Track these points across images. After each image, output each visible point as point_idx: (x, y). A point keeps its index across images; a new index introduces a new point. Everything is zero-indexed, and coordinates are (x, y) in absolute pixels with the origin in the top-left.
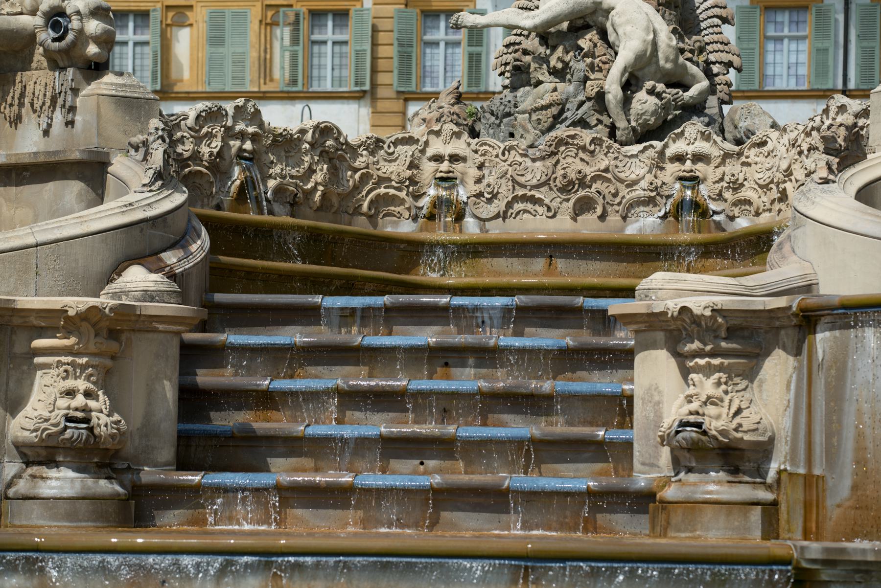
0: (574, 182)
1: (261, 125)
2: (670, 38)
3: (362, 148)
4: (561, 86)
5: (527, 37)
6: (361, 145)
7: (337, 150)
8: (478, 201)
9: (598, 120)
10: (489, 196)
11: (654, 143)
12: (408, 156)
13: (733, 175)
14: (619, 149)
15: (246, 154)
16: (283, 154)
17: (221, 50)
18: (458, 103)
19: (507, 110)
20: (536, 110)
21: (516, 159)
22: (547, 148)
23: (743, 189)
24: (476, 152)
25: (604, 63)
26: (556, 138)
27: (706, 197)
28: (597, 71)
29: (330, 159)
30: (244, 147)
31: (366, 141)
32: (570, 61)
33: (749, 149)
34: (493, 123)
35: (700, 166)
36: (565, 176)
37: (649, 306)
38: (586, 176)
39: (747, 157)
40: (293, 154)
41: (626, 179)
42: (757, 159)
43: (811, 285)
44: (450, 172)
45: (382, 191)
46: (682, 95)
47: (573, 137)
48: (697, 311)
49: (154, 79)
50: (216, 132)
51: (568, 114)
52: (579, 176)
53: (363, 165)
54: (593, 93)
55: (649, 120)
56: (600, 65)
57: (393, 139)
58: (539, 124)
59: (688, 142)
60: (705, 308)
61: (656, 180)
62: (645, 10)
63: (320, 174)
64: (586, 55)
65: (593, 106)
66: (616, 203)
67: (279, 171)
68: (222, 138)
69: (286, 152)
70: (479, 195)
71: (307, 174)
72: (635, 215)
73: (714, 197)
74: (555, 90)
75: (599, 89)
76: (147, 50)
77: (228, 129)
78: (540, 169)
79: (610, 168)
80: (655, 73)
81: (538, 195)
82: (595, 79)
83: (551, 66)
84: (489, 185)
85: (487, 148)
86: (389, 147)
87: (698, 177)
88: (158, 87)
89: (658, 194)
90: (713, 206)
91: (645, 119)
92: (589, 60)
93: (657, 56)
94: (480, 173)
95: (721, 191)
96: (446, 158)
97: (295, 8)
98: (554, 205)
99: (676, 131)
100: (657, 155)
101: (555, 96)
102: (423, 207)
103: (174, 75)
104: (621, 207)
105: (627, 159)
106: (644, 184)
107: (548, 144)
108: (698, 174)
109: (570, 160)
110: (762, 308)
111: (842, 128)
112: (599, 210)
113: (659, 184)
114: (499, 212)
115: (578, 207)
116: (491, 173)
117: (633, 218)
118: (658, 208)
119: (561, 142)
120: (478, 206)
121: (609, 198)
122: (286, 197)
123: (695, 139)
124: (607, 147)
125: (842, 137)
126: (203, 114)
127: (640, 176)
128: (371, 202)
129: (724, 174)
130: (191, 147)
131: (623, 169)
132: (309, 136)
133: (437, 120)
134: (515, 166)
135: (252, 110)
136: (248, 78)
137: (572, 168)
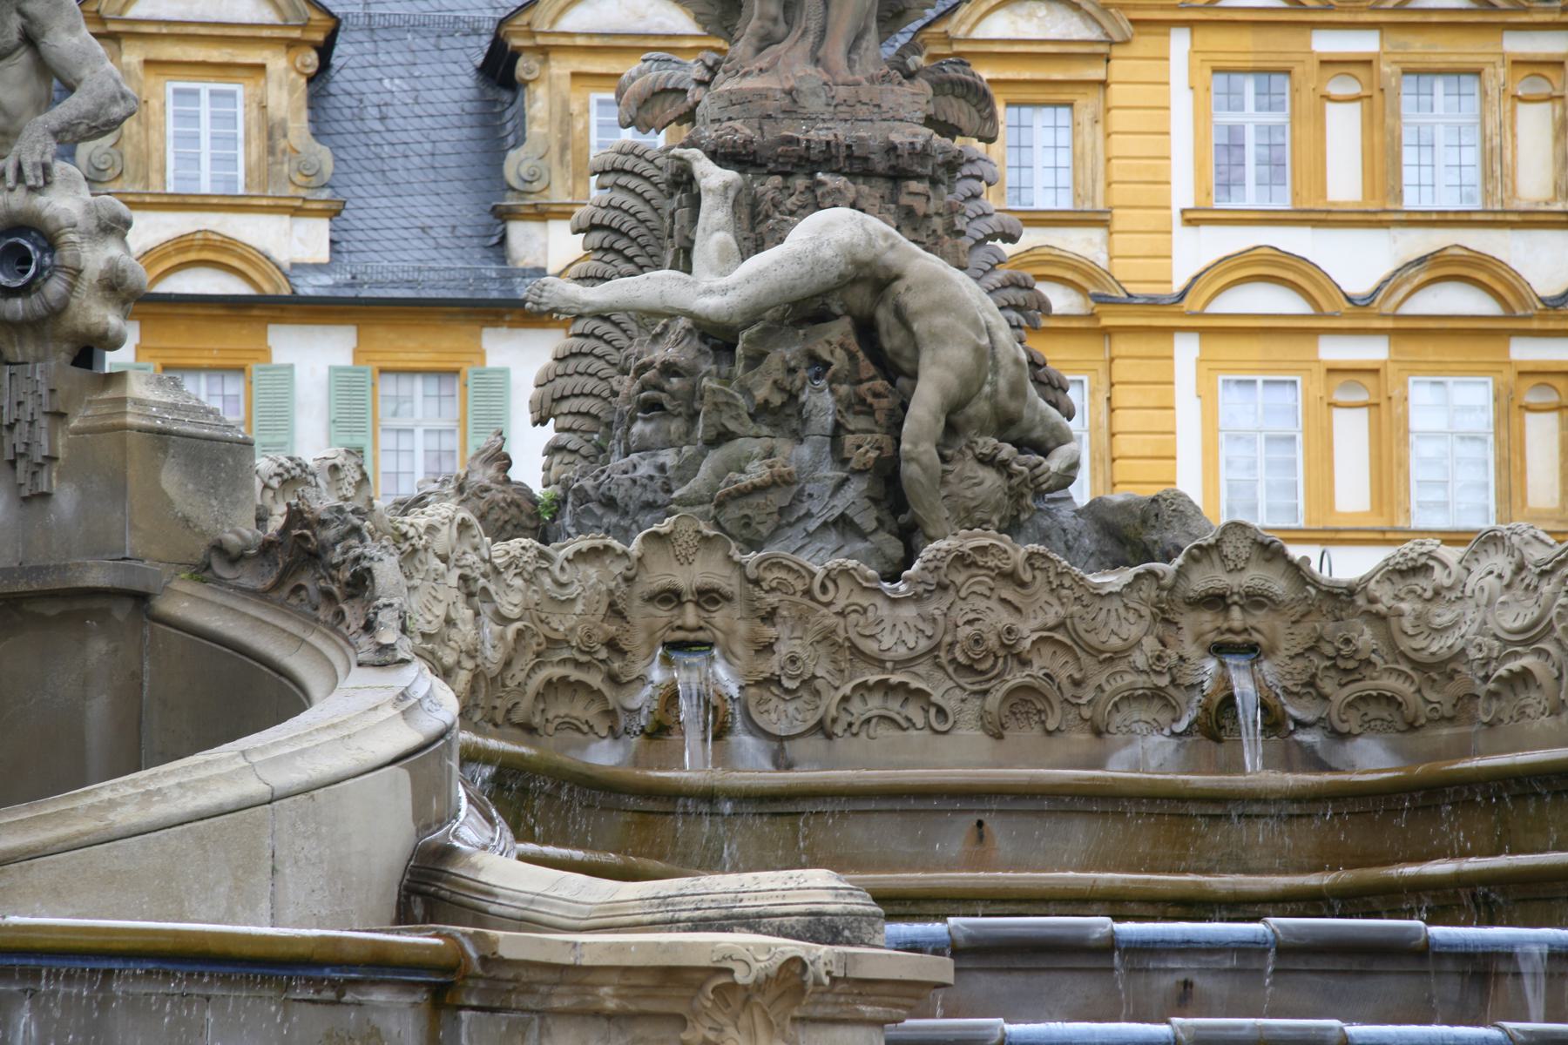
3: (512, 571)
4: (784, 446)
5: (656, 338)
6: (510, 564)
8: (767, 695)
9: (878, 519)
11: (1158, 566)
19: (649, 497)
27: (1278, 691)
29: (470, 595)
32: (802, 388)
35: (1260, 619)
36: (978, 641)
41: (1101, 647)
44: (701, 628)
45: (556, 672)
47: (982, 550)
56: (870, 399)
57: (569, 551)
61: (1168, 651)
65: (869, 488)
70: (773, 681)
73: (1295, 689)
74: (770, 454)
81: (915, 684)
84: (793, 660)
85: (783, 574)
87: (1257, 644)
89: (1173, 682)
92: (844, 389)
95: (1314, 676)
98: (950, 705)
105: (1098, 604)
106: (1140, 660)
107: (931, 565)
108: (1257, 637)
109: (982, 604)
113: (1174, 660)
117: (1119, 736)
119: (962, 560)
120: (766, 708)
129: (1320, 638)
134: (854, 616)
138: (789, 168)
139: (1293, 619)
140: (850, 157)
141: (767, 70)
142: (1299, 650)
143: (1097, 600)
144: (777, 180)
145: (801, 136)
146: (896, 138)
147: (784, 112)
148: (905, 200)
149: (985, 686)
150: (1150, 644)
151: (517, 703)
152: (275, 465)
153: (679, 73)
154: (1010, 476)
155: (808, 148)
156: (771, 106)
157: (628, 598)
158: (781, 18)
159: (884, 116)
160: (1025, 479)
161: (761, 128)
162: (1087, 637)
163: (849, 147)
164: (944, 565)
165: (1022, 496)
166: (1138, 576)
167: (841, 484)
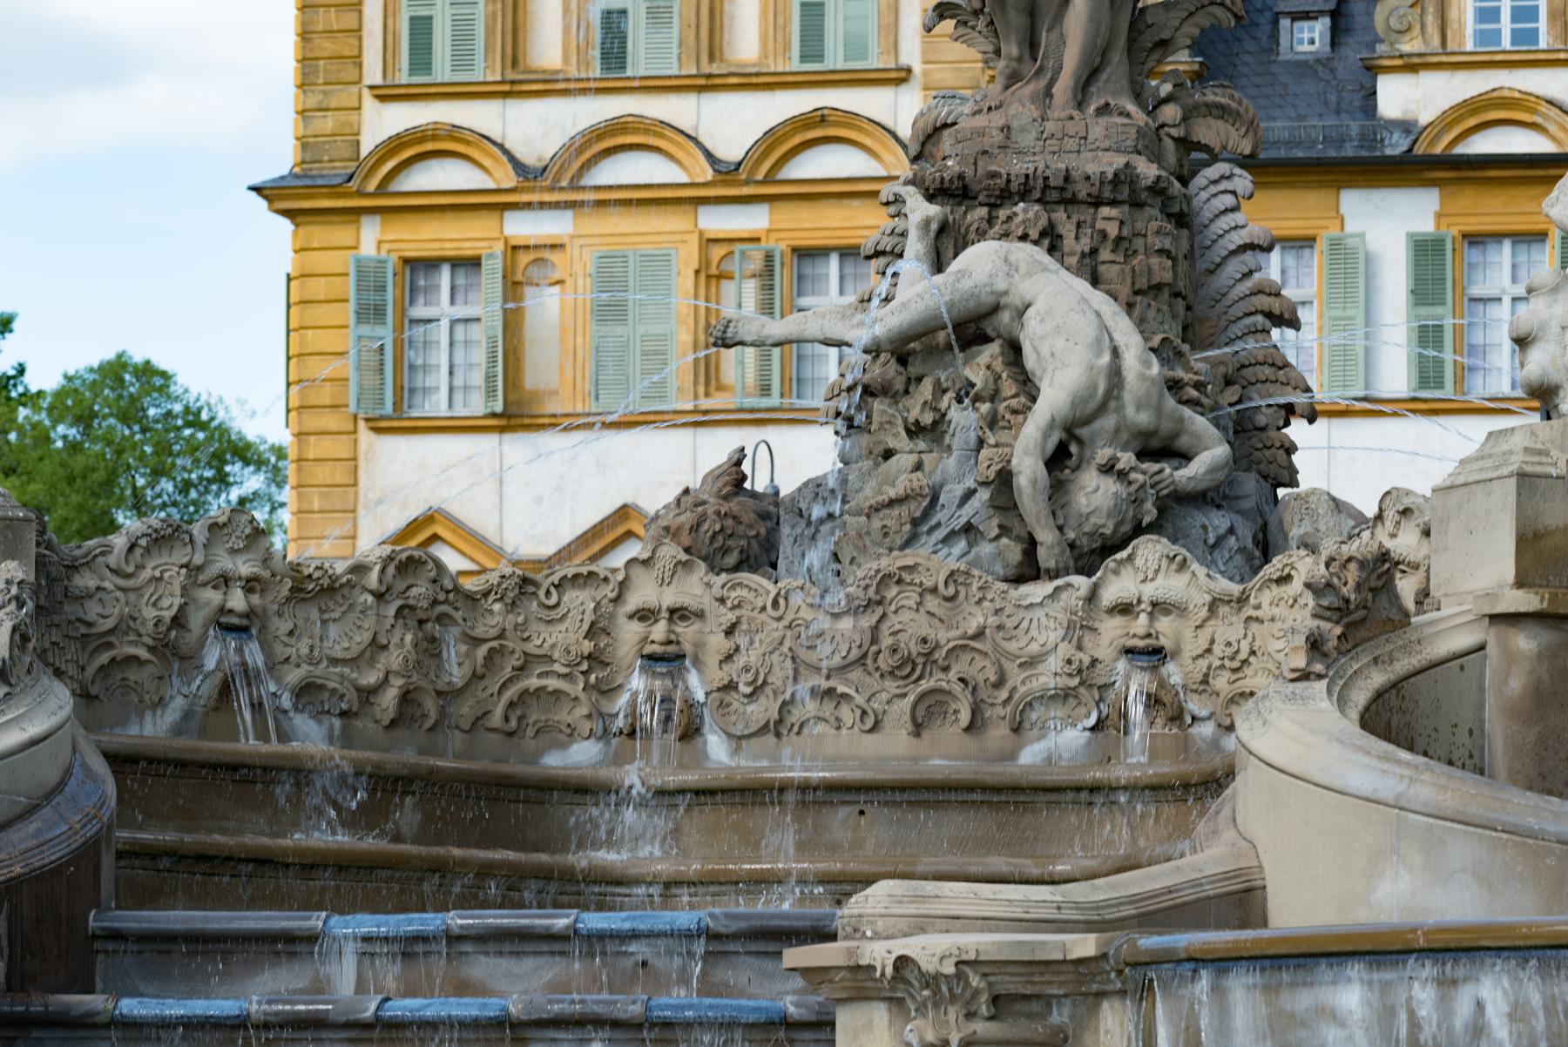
0: (913, 662)
1: (267, 560)
2: (1147, 364)
3: (492, 597)
6: (489, 592)
7: (435, 602)
9: (1000, 526)
10: (748, 690)
12: (588, 613)
13: (1229, 644)
14: (1003, 592)
15: (235, 621)
16: (314, 614)
17: (620, 330)
18: (737, 494)
20: (877, 509)
21: (801, 614)
22: (861, 593)
23: (1248, 671)
24: (722, 601)
25: (1015, 412)
26: (878, 571)
28: (1004, 428)
29: (421, 622)
30: (231, 604)
31: (499, 584)
33: (1260, 590)
34: (802, 534)
35: (1165, 624)
37: (851, 953)
38: (937, 646)
39: (1258, 607)
40: (333, 615)
41: (1018, 653)
42: (1276, 611)
43: (1248, 890)
44: (670, 642)
45: (533, 682)
46: (1172, 475)
48: (929, 965)
49: (490, 392)
50: (170, 577)
51: (940, 516)
52: (926, 649)
53: (493, 632)
54: (991, 474)
55: (1103, 526)
56: (1008, 416)
57: (556, 578)
58: (886, 535)
59: (1142, 577)
60: (942, 959)
61: (1081, 655)
62: (1096, 306)
63: (395, 654)
64: (977, 399)
66: (999, 700)
67: (305, 651)
68: (184, 588)
69: (322, 611)
70: (730, 687)
71: (368, 654)
72: (1039, 724)
73: (1195, 687)
74: (918, 467)
75: (1000, 466)
76: (476, 332)
77: (193, 570)
78: (847, 634)
79: (987, 631)
80: (1117, 431)
81: (841, 689)
82: (997, 445)
83: (911, 420)
84: (747, 669)
85: (744, 593)
86: (548, 593)
88: (499, 408)
89: (1082, 683)
90: (1194, 705)
91: (1095, 525)
92: (985, 407)
93: (1119, 398)
94: (728, 645)
95: (1206, 675)
96: (665, 614)
97: (763, 244)
99: (1118, 556)
100: (1080, 603)
101: (920, 480)
102: (618, 713)
103: (530, 381)
104: (1009, 709)
105: (1022, 613)
106: (1054, 663)
107: (863, 583)
108: (1163, 641)
109: (905, 616)
110: (1058, 956)
111: (1353, 566)
112: (965, 717)
113: (1087, 661)
114: (768, 721)
115: (921, 712)
116: (752, 642)
117: (1035, 731)
118: (1083, 710)
119: (885, 579)
121: (983, 693)
122: (322, 702)
123: (1157, 571)
124: (981, 588)
125: (1351, 584)
126: (143, 542)
127: (1050, 646)
128: (511, 704)
129: (1212, 642)
130: (116, 611)
131: (1014, 633)
132: (373, 579)
133: (691, 529)
135: (248, 531)
136: (674, 384)
137: (910, 631)
138: (993, 200)
139: (1197, 623)
140: (1046, 187)
141: (997, 108)
142: (1200, 651)
143: (1021, 610)
144: (983, 212)
145: (1003, 171)
146: (1092, 169)
147: (999, 147)
148: (1100, 225)
149: (905, 690)
150: (1065, 650)
151: (489, 712)
152: (145, 527)
153: (960, 109)
154: (1130, 483)
155: (1009, 181)
156: (987, 143)
157: (612, 616)
158: (1027, 56)
159: (1090, 147)
160: (1143, 486)
161: (975, 163)
162: (1006, 645)
163: (1046, 178)
164: (875, 583)
165: (1143, 501)
166: (1057, 589)
167: (969, 495)
